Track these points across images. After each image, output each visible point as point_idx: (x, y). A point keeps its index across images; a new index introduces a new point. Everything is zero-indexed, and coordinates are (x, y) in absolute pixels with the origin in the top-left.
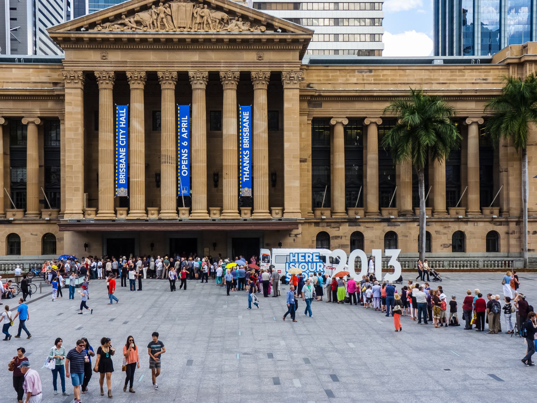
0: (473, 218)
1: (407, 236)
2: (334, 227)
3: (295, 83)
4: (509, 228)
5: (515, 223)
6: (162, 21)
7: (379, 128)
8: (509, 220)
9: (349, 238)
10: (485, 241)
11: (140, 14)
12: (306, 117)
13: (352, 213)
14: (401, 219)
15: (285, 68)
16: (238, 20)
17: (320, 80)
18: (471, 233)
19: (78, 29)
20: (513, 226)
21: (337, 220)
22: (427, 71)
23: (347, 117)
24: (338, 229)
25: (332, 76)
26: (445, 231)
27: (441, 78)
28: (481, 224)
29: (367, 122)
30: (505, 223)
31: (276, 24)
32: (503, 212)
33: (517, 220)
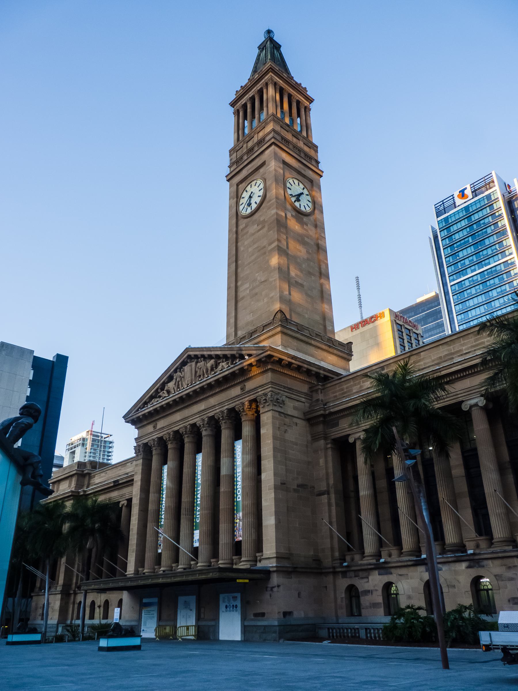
1: (454, 586)
2: (362, 578)
3: (268, 405)
6: (178, 385)
9: (380, 592)
11: (169, 384)
12: (322, 442)
15: (260, 393)
16: (223, 362)
17: (336, 396)
19: (138, 410)
22: (445, 346)
24: (366, 580)
25: (347, 388)
26: (510, 574)
27: (464, 348)
31: (244, 352)
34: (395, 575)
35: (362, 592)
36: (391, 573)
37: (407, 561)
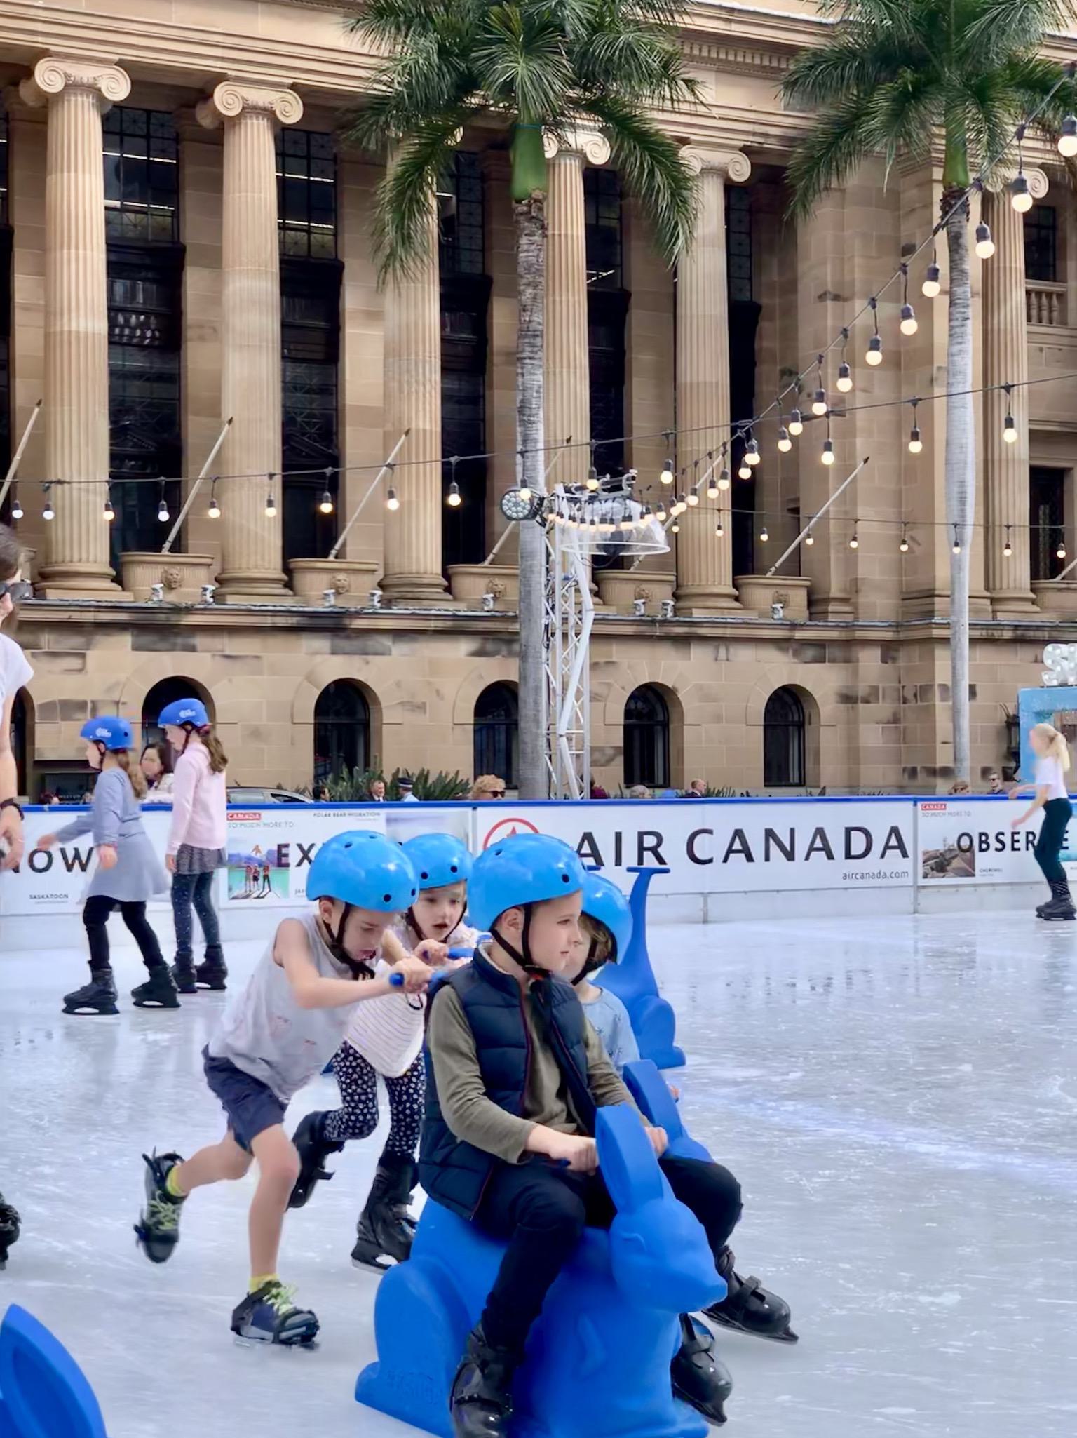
0: (713, 624)
1: (422, 707)
4: (855, 673)
5: (877, 653)
7: (285, 137)
8: (859, 634)
10: (760, 732)
13: (149, 580)
14: (400, 615)
18: (706, 696)
20: (870, 660)
21: (77, 616)
23: (121, 63)
24: (75, 663)
28: (744, 654)
29: (225, 100)
30: (837, 652)
32: (827, 601)
33: (889, 635)
34: (208, 655)
35: (49, 707)
36: (193, 649)
37: (275, 613)
